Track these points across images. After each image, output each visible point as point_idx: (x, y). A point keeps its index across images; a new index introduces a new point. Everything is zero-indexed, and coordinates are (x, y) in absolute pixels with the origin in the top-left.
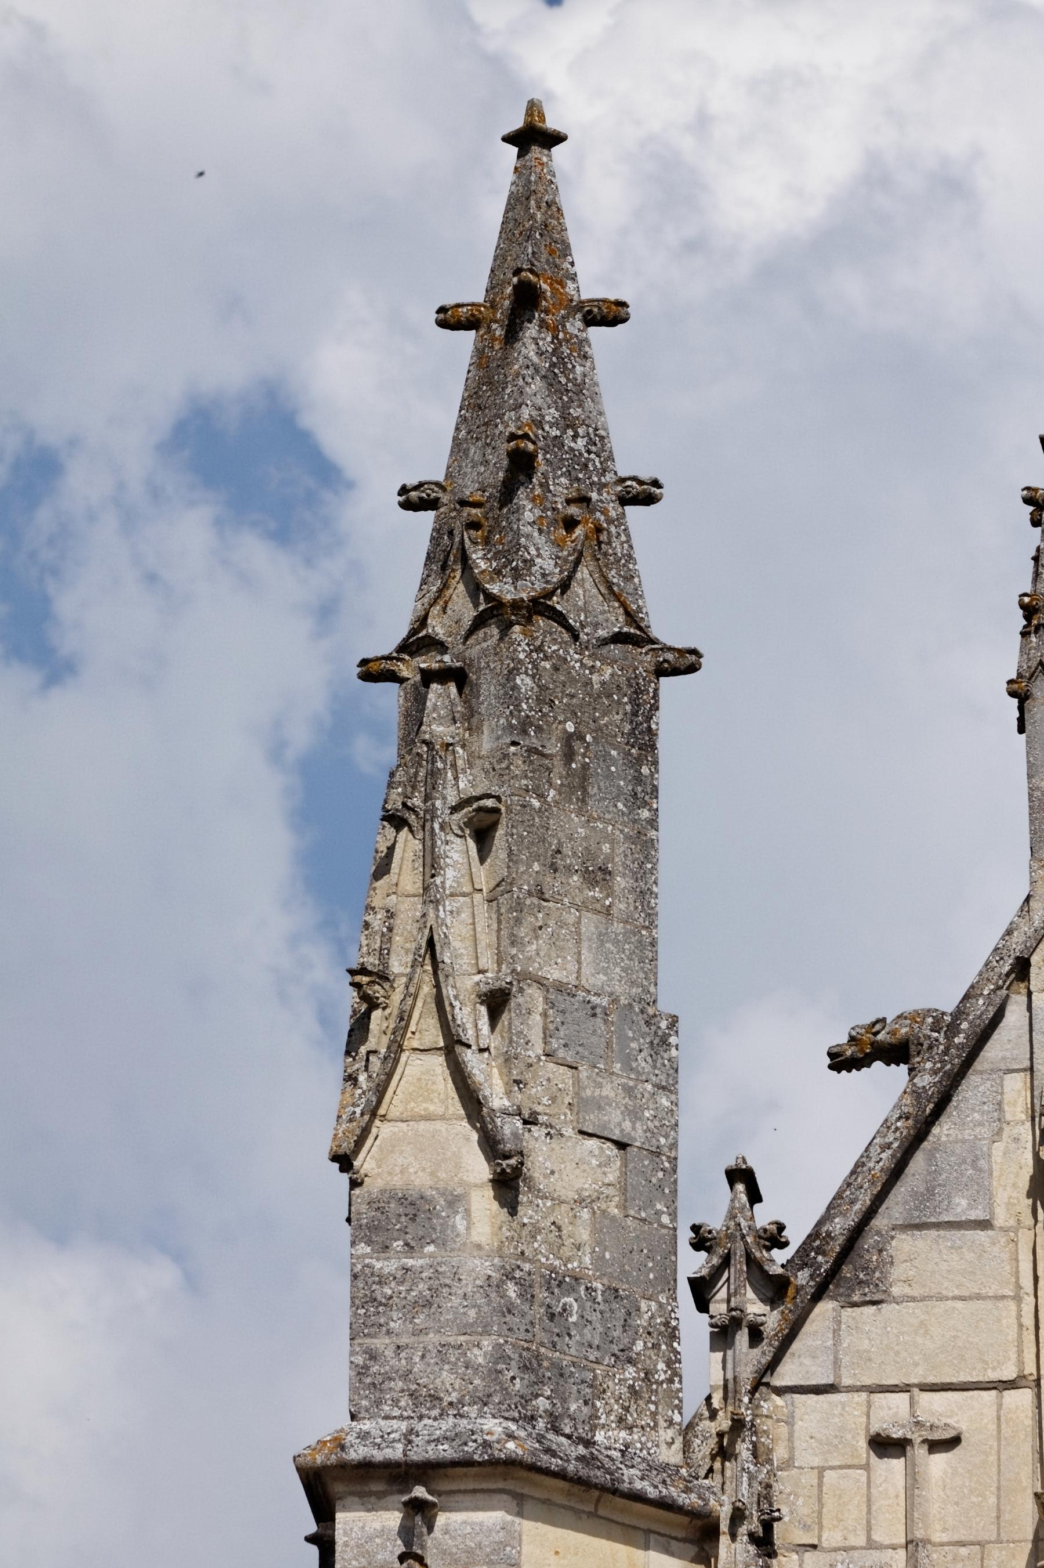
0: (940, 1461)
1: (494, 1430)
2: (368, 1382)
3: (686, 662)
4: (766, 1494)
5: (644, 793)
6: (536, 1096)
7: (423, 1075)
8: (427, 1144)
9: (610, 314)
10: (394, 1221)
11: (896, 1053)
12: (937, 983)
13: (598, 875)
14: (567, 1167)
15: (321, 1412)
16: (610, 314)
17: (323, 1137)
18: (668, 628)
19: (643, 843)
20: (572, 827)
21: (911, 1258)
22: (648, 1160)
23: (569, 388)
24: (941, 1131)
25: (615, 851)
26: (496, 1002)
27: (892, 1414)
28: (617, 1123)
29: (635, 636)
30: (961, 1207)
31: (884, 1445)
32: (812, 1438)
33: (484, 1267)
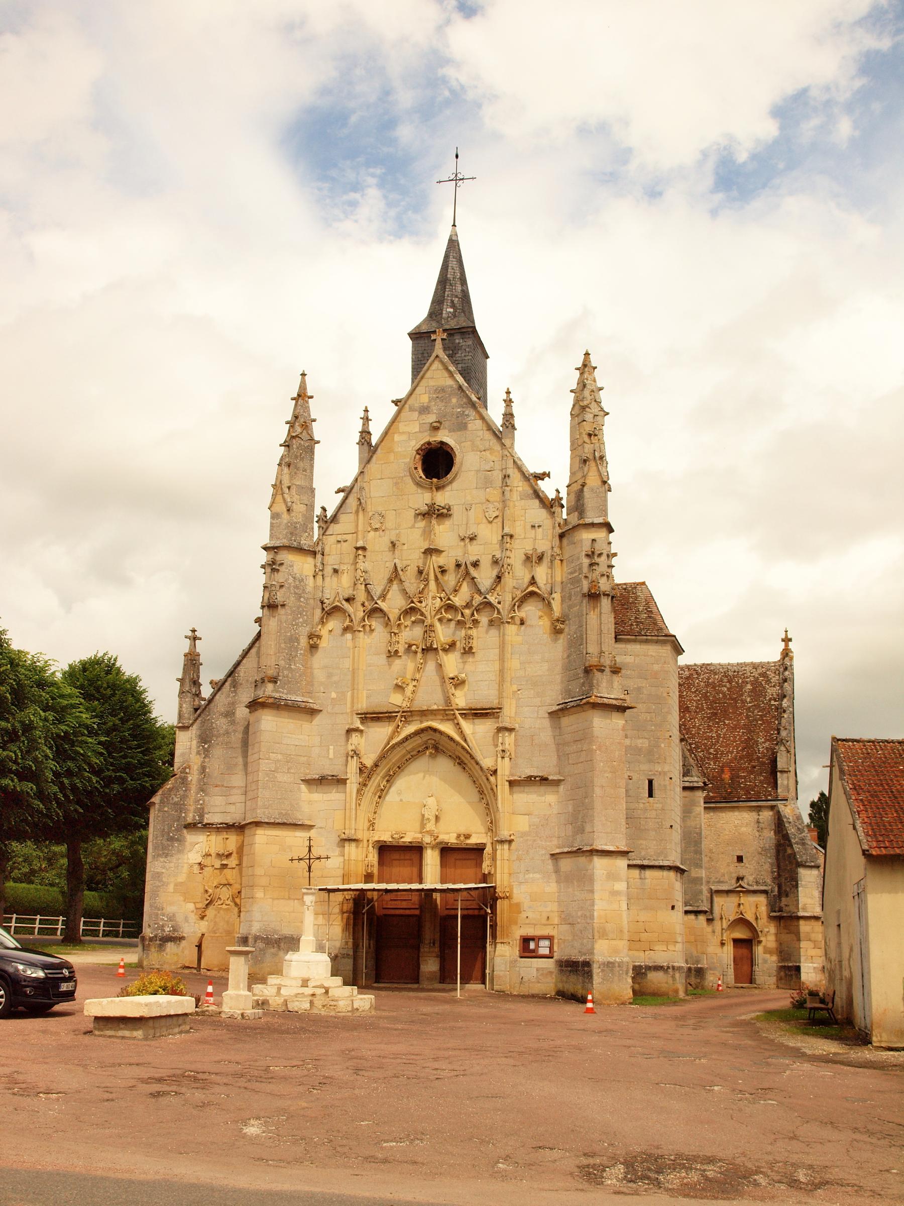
0: (345, 544)
1: (285, 542)
2: (272, 536)
3: (318, 442)
4: (323, 549)
5: (312, 459)
6: (294, 499)
7: (279, 497)
8: (280, 508)
9: (312, 397)
10: (275, 516)
11: (343, 491)
12: (348, 483)
13: (305, 470)
14: (299, 508)
15: (266, 541)
16: (312, 397)
17: (268, 506)
18: (316, 438)
19: (312, 466)
20: (301, 465)
21: (342, 518)
22: (311, 507)
23: (307, 409)
24: (347, 501)
25: (308, 468)
26: (289, 488)
27: (339, 538)
28: (306, 502)
29: (312, 439)
30: (349, 511)
31: (339, 541)
32: (330, 541)
33: (285, 521)
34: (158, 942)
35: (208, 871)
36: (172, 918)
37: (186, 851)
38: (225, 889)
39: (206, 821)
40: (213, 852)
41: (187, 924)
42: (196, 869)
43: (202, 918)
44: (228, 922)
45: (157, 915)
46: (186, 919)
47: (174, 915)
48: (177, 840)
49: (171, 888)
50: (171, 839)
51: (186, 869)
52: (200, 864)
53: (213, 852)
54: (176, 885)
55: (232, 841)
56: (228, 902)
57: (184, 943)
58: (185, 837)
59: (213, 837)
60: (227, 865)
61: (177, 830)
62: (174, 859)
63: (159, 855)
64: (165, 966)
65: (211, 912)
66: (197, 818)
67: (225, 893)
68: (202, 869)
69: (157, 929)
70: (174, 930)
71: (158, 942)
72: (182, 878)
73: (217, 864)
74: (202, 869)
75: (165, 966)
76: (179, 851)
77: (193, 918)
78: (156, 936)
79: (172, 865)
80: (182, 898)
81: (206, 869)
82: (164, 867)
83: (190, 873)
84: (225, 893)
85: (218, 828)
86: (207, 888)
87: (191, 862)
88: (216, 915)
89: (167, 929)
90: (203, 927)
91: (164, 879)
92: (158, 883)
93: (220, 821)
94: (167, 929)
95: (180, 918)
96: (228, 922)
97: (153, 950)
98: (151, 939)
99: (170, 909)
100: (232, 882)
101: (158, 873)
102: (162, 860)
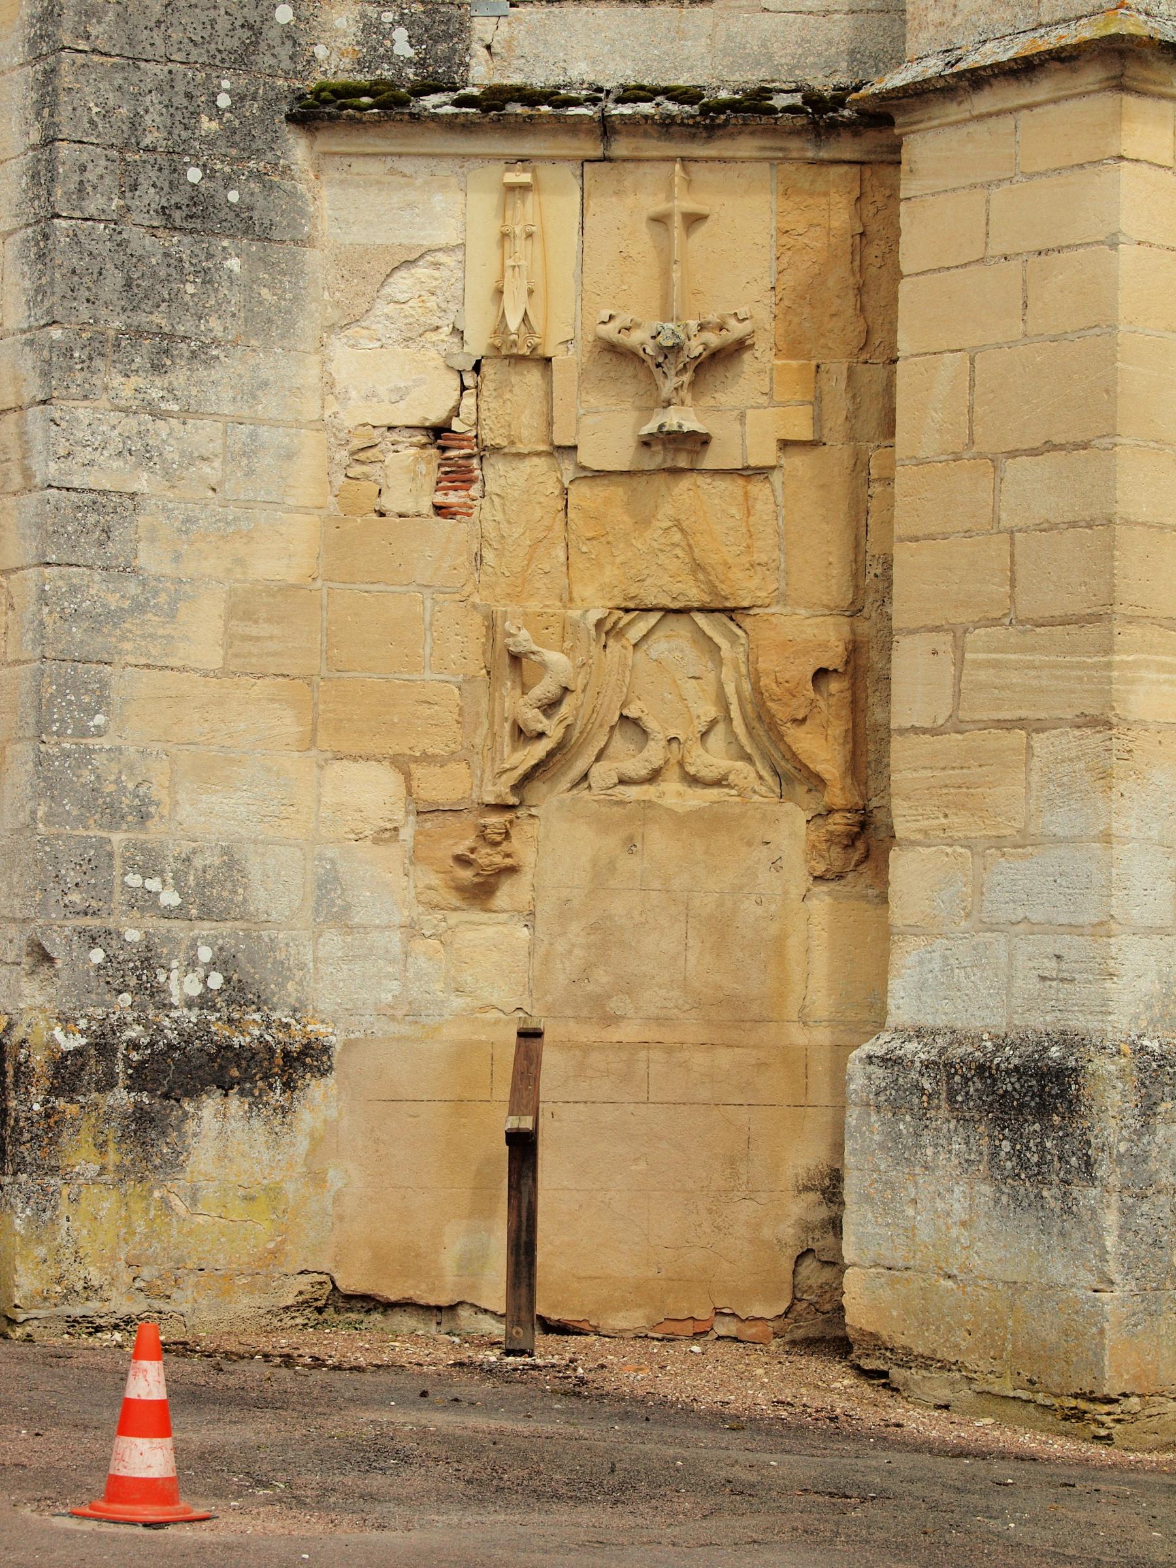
34: (121, 1098)
35: (515, 490)
36: (213, 891)
37: (308, 326)
38: (673, 645)
39: (481, 74)
40: (563, 331)
41: (333, 942)
42: (408, 477)
43: (481, 890)
44: (720, 930)
45: (97, 862)
46: (330, 902)
47: (232, 863)
48: (248, 225)
49: (201, 636)
50: (194, 214)
51: (309, 476)
52: (438, 433)
53: (563, 331)
54: (241, 609)
55: (748, 236)
56: (712, 758)
57: (320, 1099)
58: (297, 209)
59: (558, 203)
60: (700, 441)
61: (241, 138)
62: (220, 384)
63: (101, 348)
64: (182, 1301)
65: (558, 843)
66: (402, 46)
67: (678, 682)
68: (458, 476)
69: (112, 976)
70: (240, 994)
71: (121, 1098)
72: (283, 552)
73: (609, 430)
74: (458, 476)
75: (182, 1301)
76: (267, 325)
77: (390, 887)
78: (103, 1047)
79: (204, 434)
80: (288, 724)
81: (497, 475)
82: (147, 456)
83: (359, 511)
84: (678, 682)
85: (606, 128)
86: (524, 640)
87: (355, 413)
88: (602, 875)
89: (183, 986)
90: (488, 967)
91: (149, 559)
92: (100, 591)
93: (617, 72)
94: (183, 986)
95: (276, 891)
96: (720, 930)
97: (81, 1157)
98: (67, 1074)
99: (200, 816)
100: (745, 588)
101: (97, 499)
102: (125, 387)
